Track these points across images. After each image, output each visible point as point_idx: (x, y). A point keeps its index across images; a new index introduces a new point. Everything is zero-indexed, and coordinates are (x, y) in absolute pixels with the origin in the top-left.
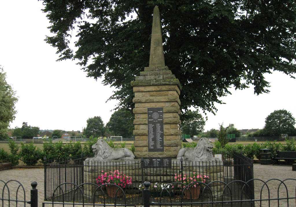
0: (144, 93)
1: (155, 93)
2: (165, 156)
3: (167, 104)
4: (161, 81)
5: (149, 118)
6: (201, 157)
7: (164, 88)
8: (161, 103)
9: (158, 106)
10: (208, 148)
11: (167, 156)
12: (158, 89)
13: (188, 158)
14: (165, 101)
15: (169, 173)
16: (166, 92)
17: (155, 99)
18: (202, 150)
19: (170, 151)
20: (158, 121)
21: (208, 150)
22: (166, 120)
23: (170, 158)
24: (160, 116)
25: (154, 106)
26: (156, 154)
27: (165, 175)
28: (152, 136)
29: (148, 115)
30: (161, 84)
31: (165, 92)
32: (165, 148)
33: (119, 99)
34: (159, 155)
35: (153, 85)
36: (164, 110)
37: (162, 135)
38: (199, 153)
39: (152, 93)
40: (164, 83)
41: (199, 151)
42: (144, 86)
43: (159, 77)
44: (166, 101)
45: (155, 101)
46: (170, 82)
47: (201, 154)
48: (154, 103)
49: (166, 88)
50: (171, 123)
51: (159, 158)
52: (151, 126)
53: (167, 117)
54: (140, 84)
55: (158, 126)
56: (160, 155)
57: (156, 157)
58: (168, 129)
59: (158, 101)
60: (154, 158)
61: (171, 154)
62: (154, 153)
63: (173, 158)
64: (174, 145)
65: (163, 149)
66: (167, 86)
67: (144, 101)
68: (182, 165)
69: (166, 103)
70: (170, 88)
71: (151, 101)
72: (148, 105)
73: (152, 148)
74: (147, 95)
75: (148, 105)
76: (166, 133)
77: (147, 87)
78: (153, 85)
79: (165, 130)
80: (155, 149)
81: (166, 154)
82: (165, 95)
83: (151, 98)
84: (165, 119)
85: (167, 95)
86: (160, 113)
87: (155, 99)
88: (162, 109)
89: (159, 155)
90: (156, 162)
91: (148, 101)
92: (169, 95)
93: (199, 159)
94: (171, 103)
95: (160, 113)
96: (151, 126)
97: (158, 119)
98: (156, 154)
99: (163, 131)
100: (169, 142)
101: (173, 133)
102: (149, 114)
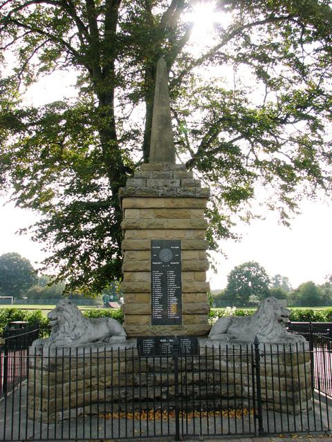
0: (143, 212)
1: (165, 211)
2: (184, 332)
3: (190, 234)
4: (179, 190)
5: (153, 259)
6: (269, 333)
7: (183, 203)
8: (177, 231)
9: (170, 238)
10: (282, 316)
11: (189, 334)
12: (172, 206)
13: (235, 336)
14: (184, 227)
15: (197, 367)
16: (186, 210)
17: (166, 223)
18: (272, 321)
19: (194, 323)
20: (170, 265)
21: (280, 321)
22: (185, 265)
23: (194, 338)
24: (174, 256)
25: (164, 237)
26: (166, 330)
27: (189, 371)
28: (159, 295)
29: (152, 254)
30: (178, 195)
31: (184, 210)
32: (185, 318)
33: (215, 240)
34: (172, 331)
35: (163, 197)
36: (182, 245)
37: (178, 294)
38: (264, 326)
39: (160, 212)
40: (183, 193)
41: (265, 322)
42: (145, 197)
43: (172, 183)
44: (187, 227)
45: (166, 227)
46: (194, 192)
47: (270, 329)
48: (164, 231)
49: (187, 203)
50: (196, 269)
51: (172, 337)
52: (158, 274)
53: (188, 258)
54: (138, 193)
55: (172, 275)
56: (176, 331)
57: (167, 334)
58: (188, 281)
59: (171, 226)
60: (163, 337)
61: (197, 329)
62: (162, 327)
63: (199, 336)
64: (202, 312)
65: (180, 319)
66: (189, 200)
67: (144, 227)
68: (257, 351)
69: (187, 232)
70: (194, 204)
71: (159, 227)
72: (152, 235)
73: (159, 317)
74: (151, 214)
75: (152, 235)
76: (186, 288)
77: (151, 200)
78: (163, 196)
79: (184, 284)
80: (165, 321)
81: (188, 328)
82: (184, 217)
83: (159, 221)
84: (186, 262)
85: (188, 217)
86: (174, 251)
87: (166, 223)
88: (178, 243)
89: (172, 331)
90: (167, 345)
91: (152, 227)
92: (192, 216)
93: (265, 338)
94: (196, 232)
95: (174, 251)
96: (158, 274)
97: (171, 261)
98: (166, 330)
99: (180, 285)
100: (192, 307)
101: (199, 290)
102: (152, 251)
